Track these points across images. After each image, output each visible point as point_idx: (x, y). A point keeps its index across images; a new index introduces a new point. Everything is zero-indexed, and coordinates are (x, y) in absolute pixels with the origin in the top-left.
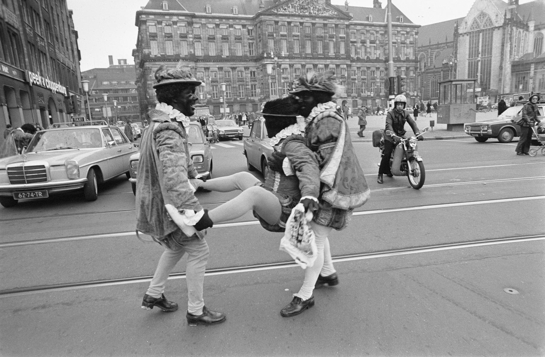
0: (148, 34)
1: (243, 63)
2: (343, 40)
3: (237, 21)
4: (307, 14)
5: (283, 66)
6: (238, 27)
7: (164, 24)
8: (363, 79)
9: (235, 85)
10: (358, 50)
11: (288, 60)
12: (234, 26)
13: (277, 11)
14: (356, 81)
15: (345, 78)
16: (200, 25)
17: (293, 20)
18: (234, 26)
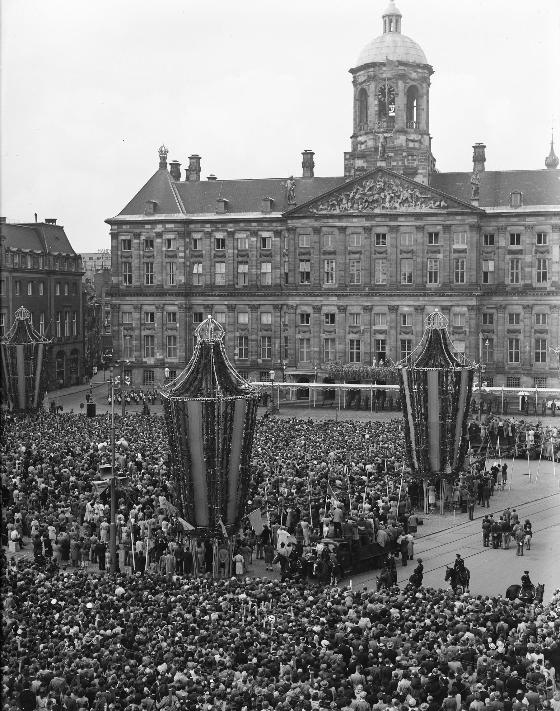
0: (119, 253)
1: (270, 298)
2: (463, 255)
3: (266, 224)
4: (377, 211)
5: (325, 310)
6: (265, 235)
7: (143, 237)
8: (536, 331)
9: (254, 337)
10: (528, 269)
11: (335, 298)
12: (260, 233)
13: (317, 210)
14: (521, 337)
15: (464, 333)
16: (202, 234)
17: (349, 224)
18: (260, 233)
